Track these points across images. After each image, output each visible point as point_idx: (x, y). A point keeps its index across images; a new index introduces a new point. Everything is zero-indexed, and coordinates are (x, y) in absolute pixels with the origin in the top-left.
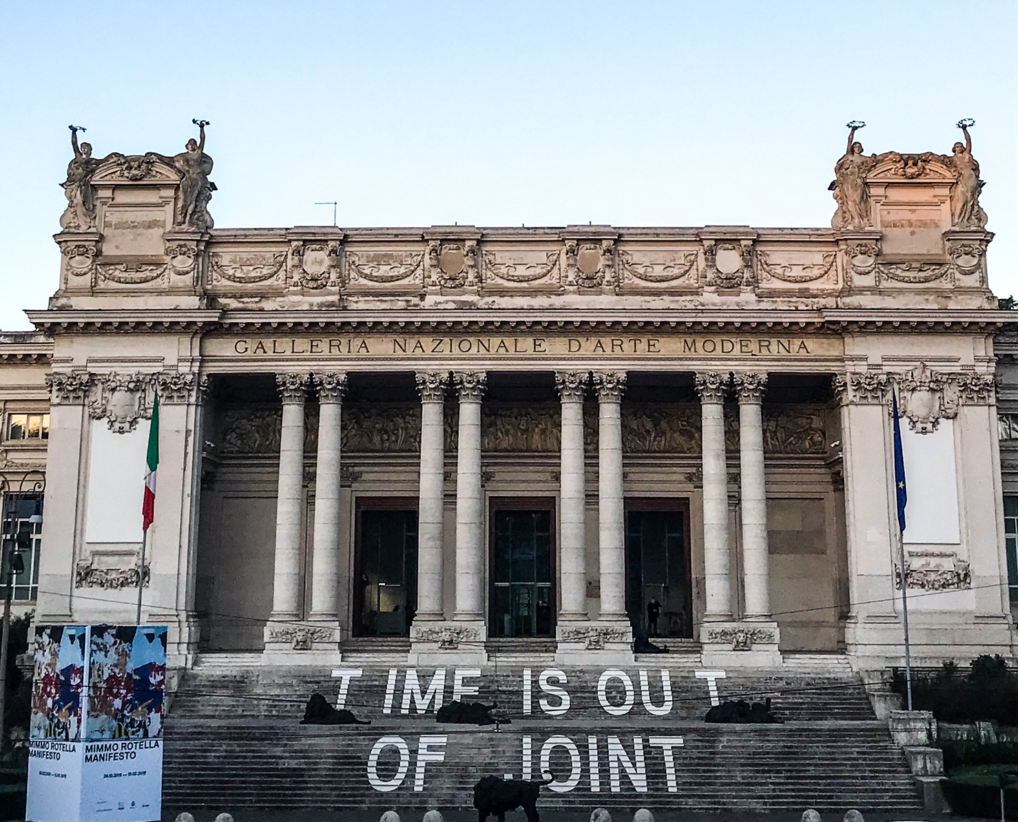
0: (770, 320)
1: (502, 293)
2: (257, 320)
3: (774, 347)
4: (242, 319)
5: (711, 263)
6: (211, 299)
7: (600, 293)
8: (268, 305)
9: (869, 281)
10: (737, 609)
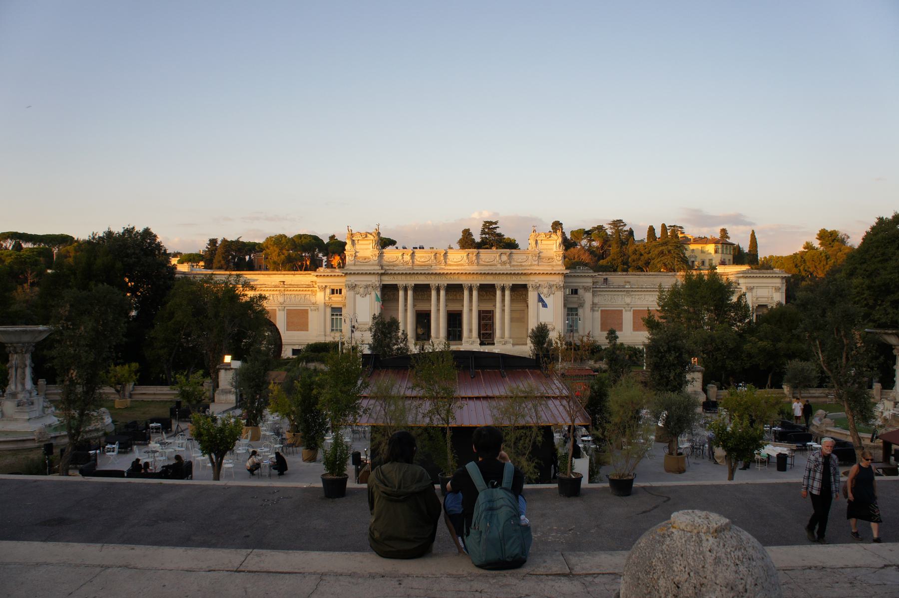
0: (513, 272)
1: (450, 265)
2: (393, 272)
3: (514, 278)
4: (390, 272)
5: (500, 258)
6: (382, 266)
7: (473, 265)
8: (395, 268)
9: (536, 263)
10: (503, 337)
